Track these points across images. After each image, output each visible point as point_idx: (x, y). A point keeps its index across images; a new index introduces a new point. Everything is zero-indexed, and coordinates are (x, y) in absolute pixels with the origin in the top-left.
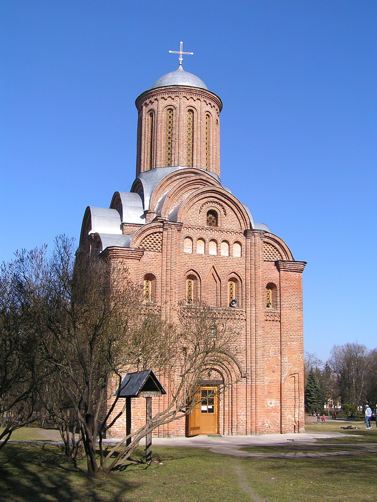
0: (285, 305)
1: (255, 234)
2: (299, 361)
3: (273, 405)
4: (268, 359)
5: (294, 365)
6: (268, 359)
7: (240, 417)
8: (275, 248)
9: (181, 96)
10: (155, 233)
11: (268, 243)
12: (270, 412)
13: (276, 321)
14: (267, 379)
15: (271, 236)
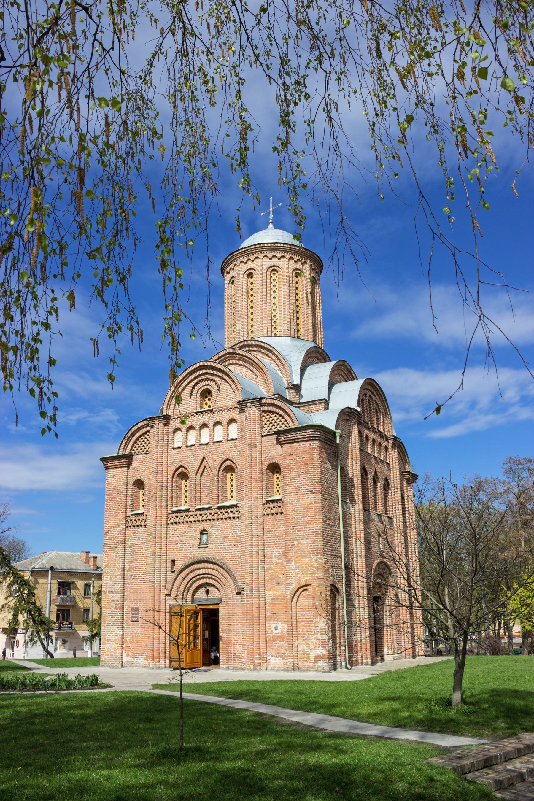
0: (290, 489)
1: (248, 404)
2: (311, 566)
3: (279, 631)
4: (270, 567)
5: (304, 572)
6: (270, 567)
7: (237, 647)
8: (281, 416)
9: (238, 262)
10: (146, 433)
11: (270, 412)
12: (276, 640)
13: (281, 513)
14: (270, 594)
15: (268, 401)
